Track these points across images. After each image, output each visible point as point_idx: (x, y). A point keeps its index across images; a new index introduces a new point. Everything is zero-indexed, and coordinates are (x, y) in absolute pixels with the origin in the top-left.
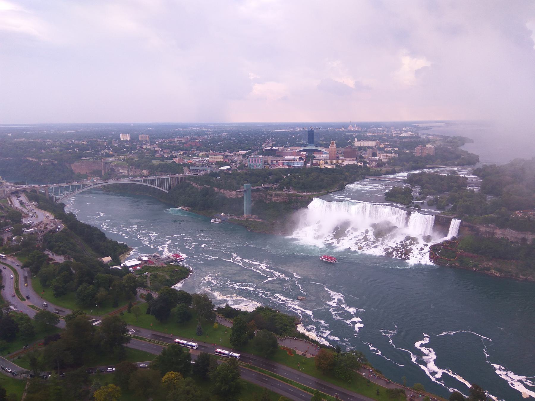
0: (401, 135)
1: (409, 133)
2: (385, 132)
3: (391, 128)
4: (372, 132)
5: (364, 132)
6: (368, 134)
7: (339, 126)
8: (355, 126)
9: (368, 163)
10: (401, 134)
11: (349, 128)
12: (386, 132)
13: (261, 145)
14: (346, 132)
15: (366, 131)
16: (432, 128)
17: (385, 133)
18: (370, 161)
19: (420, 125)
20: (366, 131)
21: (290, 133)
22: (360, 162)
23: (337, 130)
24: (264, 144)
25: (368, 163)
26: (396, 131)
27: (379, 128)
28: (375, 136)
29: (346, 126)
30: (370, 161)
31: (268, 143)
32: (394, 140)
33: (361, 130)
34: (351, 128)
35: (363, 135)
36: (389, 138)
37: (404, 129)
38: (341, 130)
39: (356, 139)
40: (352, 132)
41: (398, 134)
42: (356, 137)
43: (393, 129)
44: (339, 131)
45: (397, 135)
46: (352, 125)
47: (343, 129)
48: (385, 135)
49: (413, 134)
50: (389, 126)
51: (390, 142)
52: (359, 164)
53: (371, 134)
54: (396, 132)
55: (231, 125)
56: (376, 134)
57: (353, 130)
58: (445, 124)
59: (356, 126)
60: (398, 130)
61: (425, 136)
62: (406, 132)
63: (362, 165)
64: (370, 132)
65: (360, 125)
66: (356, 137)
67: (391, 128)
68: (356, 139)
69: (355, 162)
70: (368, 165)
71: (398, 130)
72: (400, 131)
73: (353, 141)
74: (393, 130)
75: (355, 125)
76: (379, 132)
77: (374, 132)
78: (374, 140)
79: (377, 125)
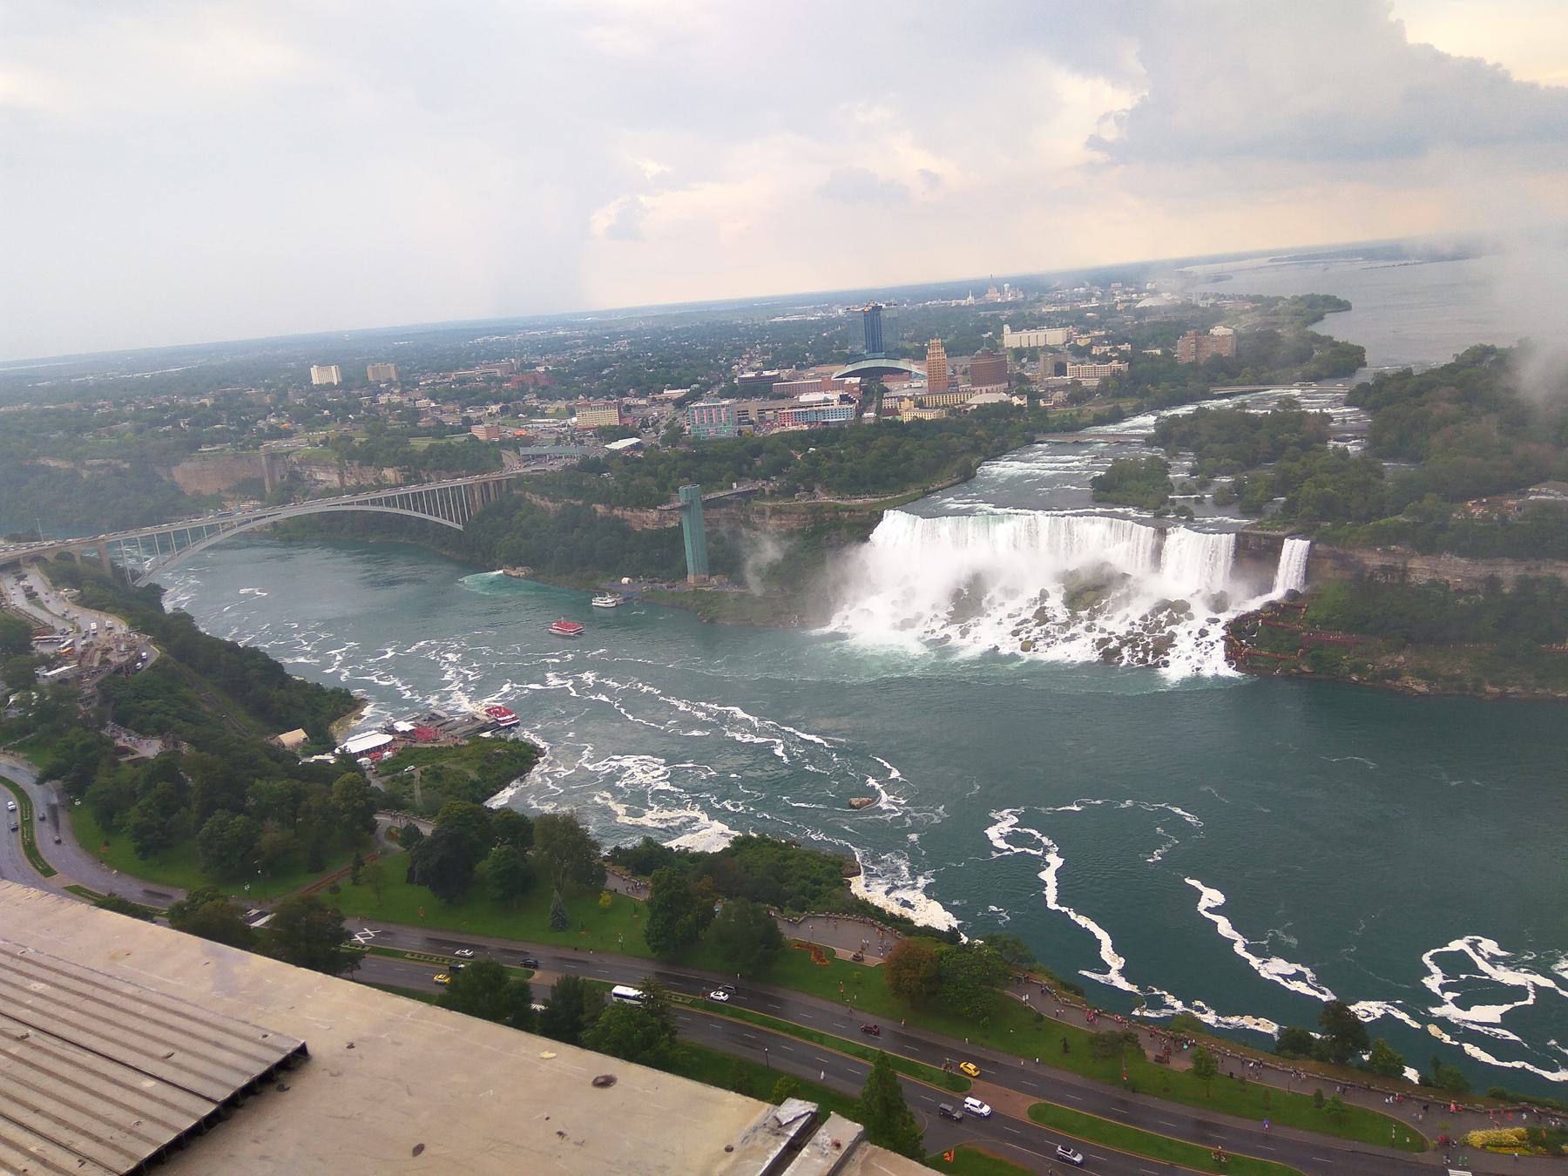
0: (1139, 306)
2: (1094, 299)
4: (1054, 303)
5: (1031, 302)
6: (1044, 310)
7: (958, 290)
8: (1006, 289)
9: (1041, 396)
10: (1141, 301)
13: (729, 368)
15: (1039, 300)
17: (1094, 303)
18: (1047, 390)
21: (813, 324)
22: (1020, 393)
23: (954, 303)
24: (738, 364)
25: (1041, 396)
26: (1126, 293)
27: (1076, 290)
28: (1063, 314)
29: (979, 289)
30: (1047, 390)
31: (751, 359)
32: (1120, 320)
33: (1025, 298)
34: (994, 296)
35: (1030, 313)
38: (963, 302)
39: (1006, 328)
40: (996, 306)
41: (1131, 301)
43: (1117, 289)
44: (958, 306)
45: (1128, 304)
46: (998, 284)
47: (971, 299)
48: (1093, 310)
50: (1105, 280)
52: (1016, 401)
53: (1053, 309)
54: (1125, 297)
55: (640, 315)
56: (1067, 308)
57: (999, 300)
58: (1271, 261)
59: (1010, 288)
60: (1132, 289)
61: (1211, 301)
63: (1024, 402)
64: (1049, 303)
67: (1113, 285)
68: (1006, 328)
69: (1004, 397)
71: (1132, 289)
72: (1138, 292)
73: (999, 334)
75: (1006, 285)
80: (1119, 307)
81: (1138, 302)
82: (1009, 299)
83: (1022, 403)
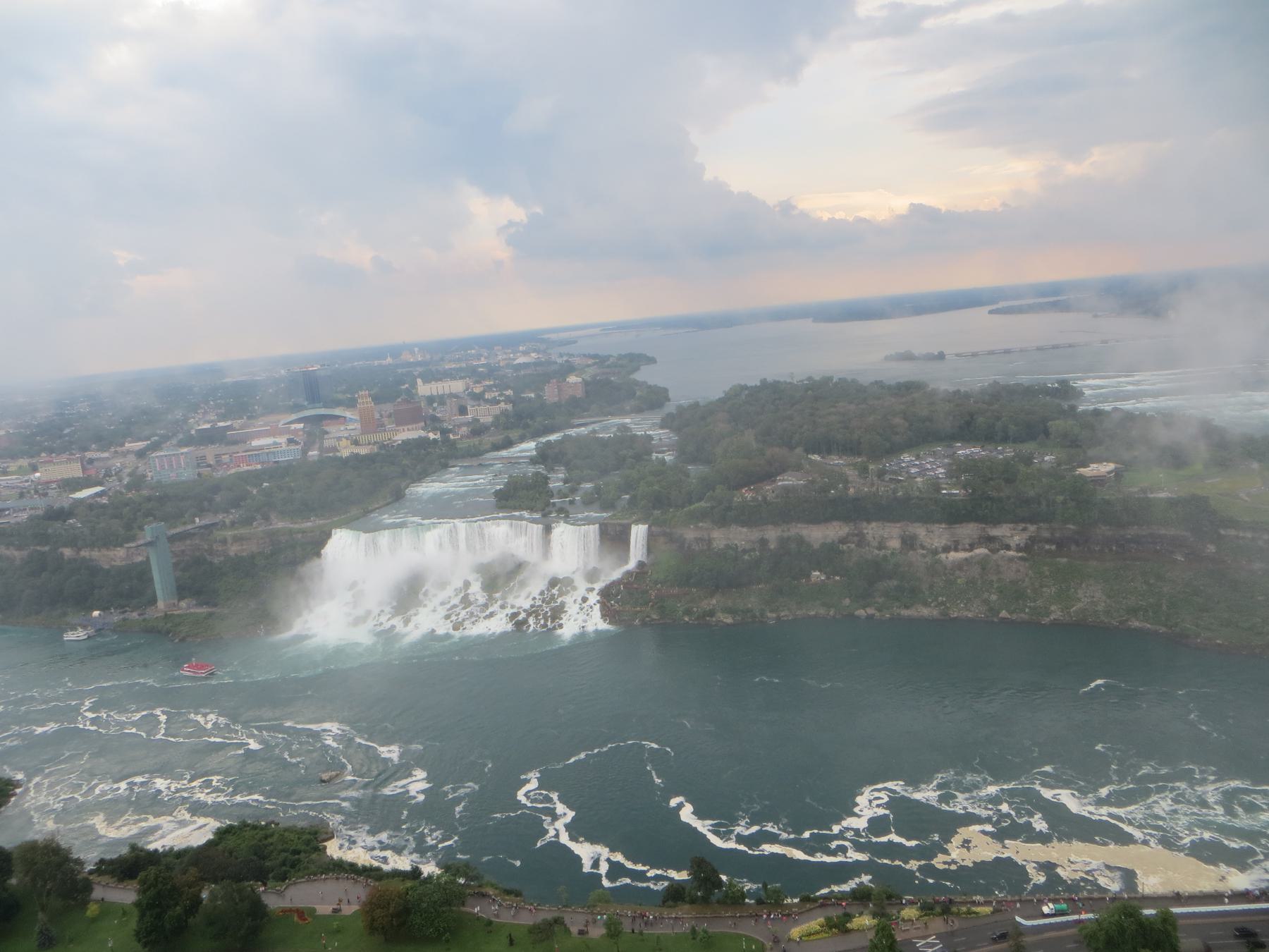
1: (533, 355)
2: (482, 359)
3: (495, 348)
7: (380, 353)
8: (416, 352)
9: (450, 431)
10: (516, 359)
11: (402, 357)
12: (485, 358)
15: (442, 360)
16: (575, 342)
17: (483, 361)
19: (553, 336)
20: (442, 360)
22: (434, 430)
23: (376, 363)
24: (194, 418)
26: (506, 353)
28: (461, 369)
29: (395, 351)
30: (454, 426)
31: (205, 413)
36: (491, 372)
37: (521, 348)
38: (384, 362)
39: (419, 381)
40: (410, 364)
41: (510, 359)
42: (420, 376)
47: (389, 360)
49: (540, 356)
50: (490, 343)
51: (495, 379)
52: (432, 436)
53: (454, 366)
54: (505, 356)
57: (412, 360)
58: (601, 330)
60: (510, 351)
61: (565, 358)
62: (525, 353)
64: (450, 361)
66: (420, 376)
67: (495, 348)
68: (419, 381)
69: (422, 433)
70: (451, 437)
71: (510, 351)
73: (414, 385)
74: (499, 353)
75: (416, 349)
76: (469, 360)
77: (459, 360)
78: (461, 378)
79: (465, 344)
80: (501, 364)
81: (514, 360)
82: (420, 359)
83: (436, 437)
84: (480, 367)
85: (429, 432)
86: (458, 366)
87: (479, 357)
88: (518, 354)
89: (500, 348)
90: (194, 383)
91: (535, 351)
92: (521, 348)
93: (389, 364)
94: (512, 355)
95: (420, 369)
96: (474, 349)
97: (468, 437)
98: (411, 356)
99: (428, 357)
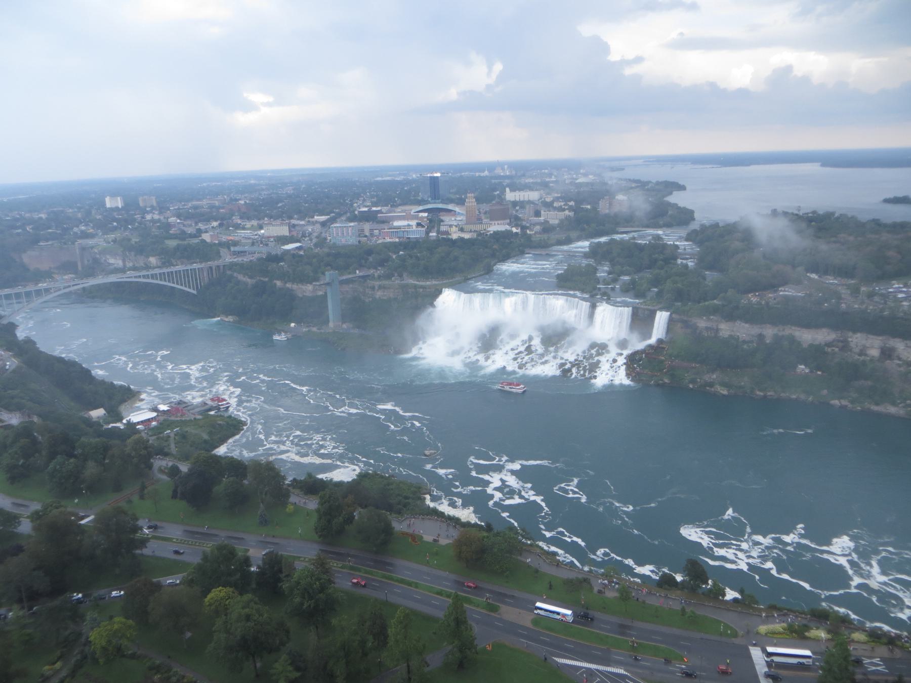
0: (577, 181)
2: (553, 177)
3: (563, 169)
4: (531, 177)
7: (480, 167)
9: (527, 228)
10: (578, 179)
11: (496, 171)
12: (555, 176)
13: (352, 205)
14: (492, 178)
16: (623, 169)
17: (553, 179)
18: (531, 224)
20: (524, 175)
22: (516, 226)
23: (477, 174)
24: (357, 203)
25: (527, 228)
26: (570, 174)
27: (543, 171)
29: (491, 167)
30: (531, 224)
31: (364, 200)
33: (516, 174)
37: (582, 171)
38: (482, 174)
39: (508, 190)
40: (500, 177)
41: (573, 179)
42: (508, 186)
44: (480, 176)
46: (501, 165)
47: (486, 173)
48: (553, 182)
52: (514, 230)
57: (502, 174)
58: (644, 162)
59: (508, 168)
61: (615, 181)
62: (586, 175)
63: (519, 231)
65: (513, 165)
66: (508, 186)
68: (508, 190)
69: (508, 227)
70: (528, 232)
71: (573, 173)
73: (503, 192)
75: (506, 167)
78: (537, 190)
79: (539, 166)
81: (577, 179)
82: (508, 174)
83: (517, 231)
84: (552, 183)
85: (512, 227)
86: (535, 181)
87: (550, 175)
88: (580, 176)
89: (567, 169)
90: (357, 179)
91: (592, 174)
92: (582, 171)
93: (486, 176)
94: (574, 176)
95: (507, 181)
96: (547, 169)
97: (540, 233)
98: (501, 171)
99: (514, 173)
